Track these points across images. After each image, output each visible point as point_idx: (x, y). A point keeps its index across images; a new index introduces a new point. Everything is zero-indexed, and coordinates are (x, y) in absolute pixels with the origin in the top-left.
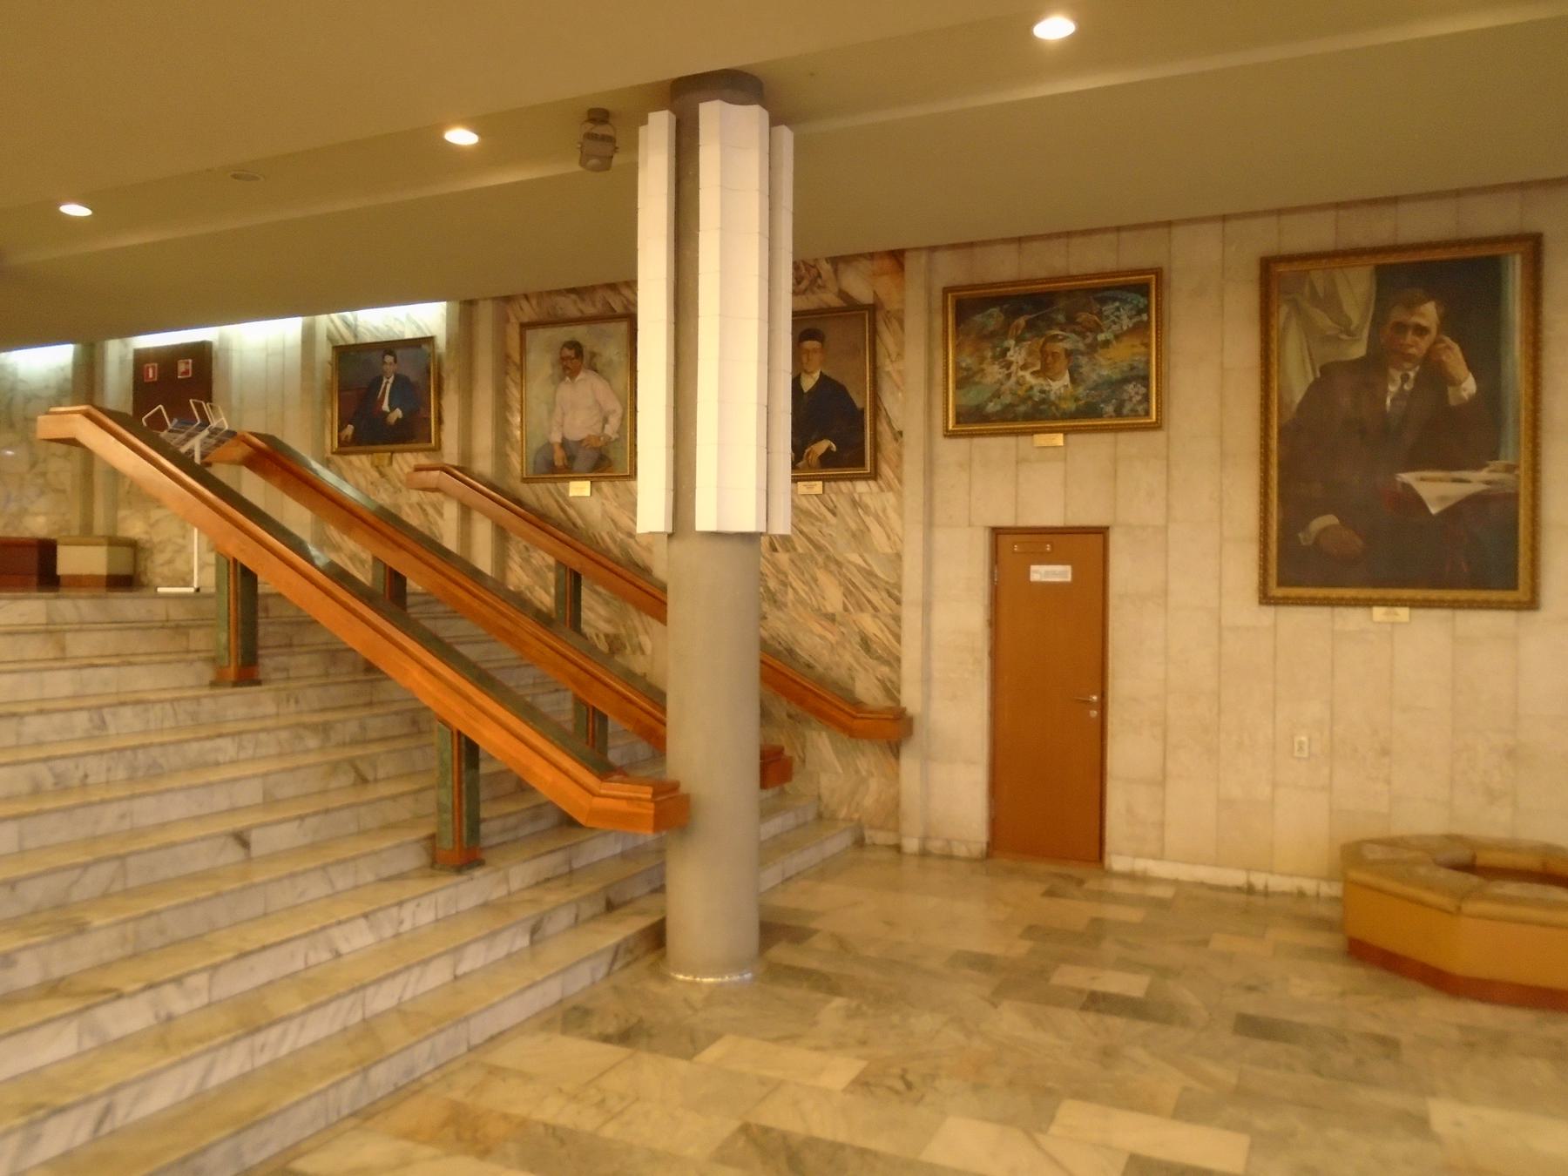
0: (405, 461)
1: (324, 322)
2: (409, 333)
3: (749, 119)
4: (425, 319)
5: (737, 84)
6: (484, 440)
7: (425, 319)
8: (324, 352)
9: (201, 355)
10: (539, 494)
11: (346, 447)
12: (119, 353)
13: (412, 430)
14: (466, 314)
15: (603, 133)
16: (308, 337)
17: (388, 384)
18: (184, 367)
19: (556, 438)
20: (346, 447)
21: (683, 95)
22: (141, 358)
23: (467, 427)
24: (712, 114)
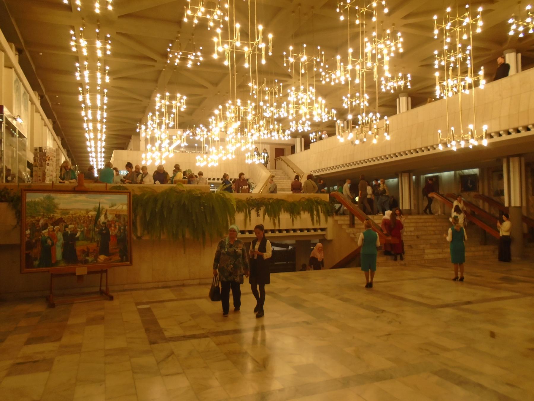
0: (473, 194)
1: (458, 172)
2: (472, 173)
3: (516, 159)
4: (476, 171)
5: (513, 156)
6: (486, 190)
7: (476, 171)
8: (458, 176)
9: (437, 177)
10: (495, 198)
11: (462, 191)
12: (423, 177)
13: (474, 188)
14: (482, 172)
15: (499, 160)
16: (455, 174)
17: (469, 181)
18: (434, 179)
19: (499, 189)
20: (462, 191)
21: (508, 158)
22: (427, 178)
23: (483, 188)
24: (511, 159)
